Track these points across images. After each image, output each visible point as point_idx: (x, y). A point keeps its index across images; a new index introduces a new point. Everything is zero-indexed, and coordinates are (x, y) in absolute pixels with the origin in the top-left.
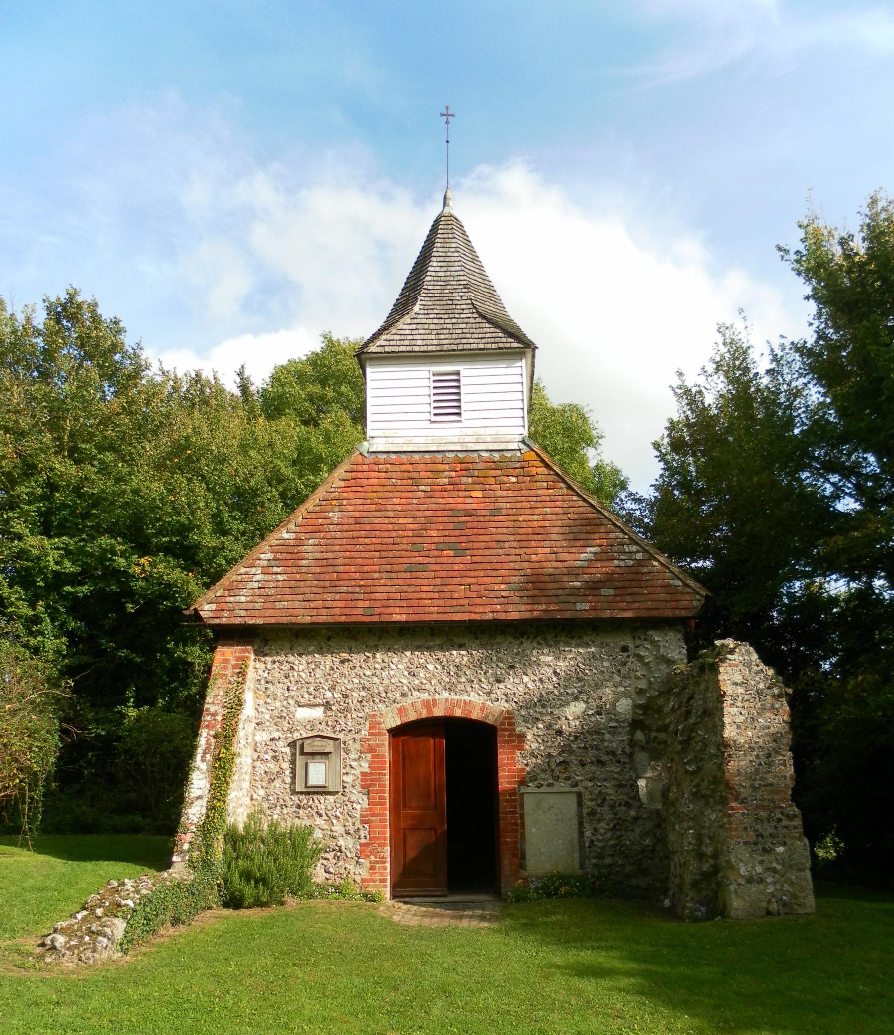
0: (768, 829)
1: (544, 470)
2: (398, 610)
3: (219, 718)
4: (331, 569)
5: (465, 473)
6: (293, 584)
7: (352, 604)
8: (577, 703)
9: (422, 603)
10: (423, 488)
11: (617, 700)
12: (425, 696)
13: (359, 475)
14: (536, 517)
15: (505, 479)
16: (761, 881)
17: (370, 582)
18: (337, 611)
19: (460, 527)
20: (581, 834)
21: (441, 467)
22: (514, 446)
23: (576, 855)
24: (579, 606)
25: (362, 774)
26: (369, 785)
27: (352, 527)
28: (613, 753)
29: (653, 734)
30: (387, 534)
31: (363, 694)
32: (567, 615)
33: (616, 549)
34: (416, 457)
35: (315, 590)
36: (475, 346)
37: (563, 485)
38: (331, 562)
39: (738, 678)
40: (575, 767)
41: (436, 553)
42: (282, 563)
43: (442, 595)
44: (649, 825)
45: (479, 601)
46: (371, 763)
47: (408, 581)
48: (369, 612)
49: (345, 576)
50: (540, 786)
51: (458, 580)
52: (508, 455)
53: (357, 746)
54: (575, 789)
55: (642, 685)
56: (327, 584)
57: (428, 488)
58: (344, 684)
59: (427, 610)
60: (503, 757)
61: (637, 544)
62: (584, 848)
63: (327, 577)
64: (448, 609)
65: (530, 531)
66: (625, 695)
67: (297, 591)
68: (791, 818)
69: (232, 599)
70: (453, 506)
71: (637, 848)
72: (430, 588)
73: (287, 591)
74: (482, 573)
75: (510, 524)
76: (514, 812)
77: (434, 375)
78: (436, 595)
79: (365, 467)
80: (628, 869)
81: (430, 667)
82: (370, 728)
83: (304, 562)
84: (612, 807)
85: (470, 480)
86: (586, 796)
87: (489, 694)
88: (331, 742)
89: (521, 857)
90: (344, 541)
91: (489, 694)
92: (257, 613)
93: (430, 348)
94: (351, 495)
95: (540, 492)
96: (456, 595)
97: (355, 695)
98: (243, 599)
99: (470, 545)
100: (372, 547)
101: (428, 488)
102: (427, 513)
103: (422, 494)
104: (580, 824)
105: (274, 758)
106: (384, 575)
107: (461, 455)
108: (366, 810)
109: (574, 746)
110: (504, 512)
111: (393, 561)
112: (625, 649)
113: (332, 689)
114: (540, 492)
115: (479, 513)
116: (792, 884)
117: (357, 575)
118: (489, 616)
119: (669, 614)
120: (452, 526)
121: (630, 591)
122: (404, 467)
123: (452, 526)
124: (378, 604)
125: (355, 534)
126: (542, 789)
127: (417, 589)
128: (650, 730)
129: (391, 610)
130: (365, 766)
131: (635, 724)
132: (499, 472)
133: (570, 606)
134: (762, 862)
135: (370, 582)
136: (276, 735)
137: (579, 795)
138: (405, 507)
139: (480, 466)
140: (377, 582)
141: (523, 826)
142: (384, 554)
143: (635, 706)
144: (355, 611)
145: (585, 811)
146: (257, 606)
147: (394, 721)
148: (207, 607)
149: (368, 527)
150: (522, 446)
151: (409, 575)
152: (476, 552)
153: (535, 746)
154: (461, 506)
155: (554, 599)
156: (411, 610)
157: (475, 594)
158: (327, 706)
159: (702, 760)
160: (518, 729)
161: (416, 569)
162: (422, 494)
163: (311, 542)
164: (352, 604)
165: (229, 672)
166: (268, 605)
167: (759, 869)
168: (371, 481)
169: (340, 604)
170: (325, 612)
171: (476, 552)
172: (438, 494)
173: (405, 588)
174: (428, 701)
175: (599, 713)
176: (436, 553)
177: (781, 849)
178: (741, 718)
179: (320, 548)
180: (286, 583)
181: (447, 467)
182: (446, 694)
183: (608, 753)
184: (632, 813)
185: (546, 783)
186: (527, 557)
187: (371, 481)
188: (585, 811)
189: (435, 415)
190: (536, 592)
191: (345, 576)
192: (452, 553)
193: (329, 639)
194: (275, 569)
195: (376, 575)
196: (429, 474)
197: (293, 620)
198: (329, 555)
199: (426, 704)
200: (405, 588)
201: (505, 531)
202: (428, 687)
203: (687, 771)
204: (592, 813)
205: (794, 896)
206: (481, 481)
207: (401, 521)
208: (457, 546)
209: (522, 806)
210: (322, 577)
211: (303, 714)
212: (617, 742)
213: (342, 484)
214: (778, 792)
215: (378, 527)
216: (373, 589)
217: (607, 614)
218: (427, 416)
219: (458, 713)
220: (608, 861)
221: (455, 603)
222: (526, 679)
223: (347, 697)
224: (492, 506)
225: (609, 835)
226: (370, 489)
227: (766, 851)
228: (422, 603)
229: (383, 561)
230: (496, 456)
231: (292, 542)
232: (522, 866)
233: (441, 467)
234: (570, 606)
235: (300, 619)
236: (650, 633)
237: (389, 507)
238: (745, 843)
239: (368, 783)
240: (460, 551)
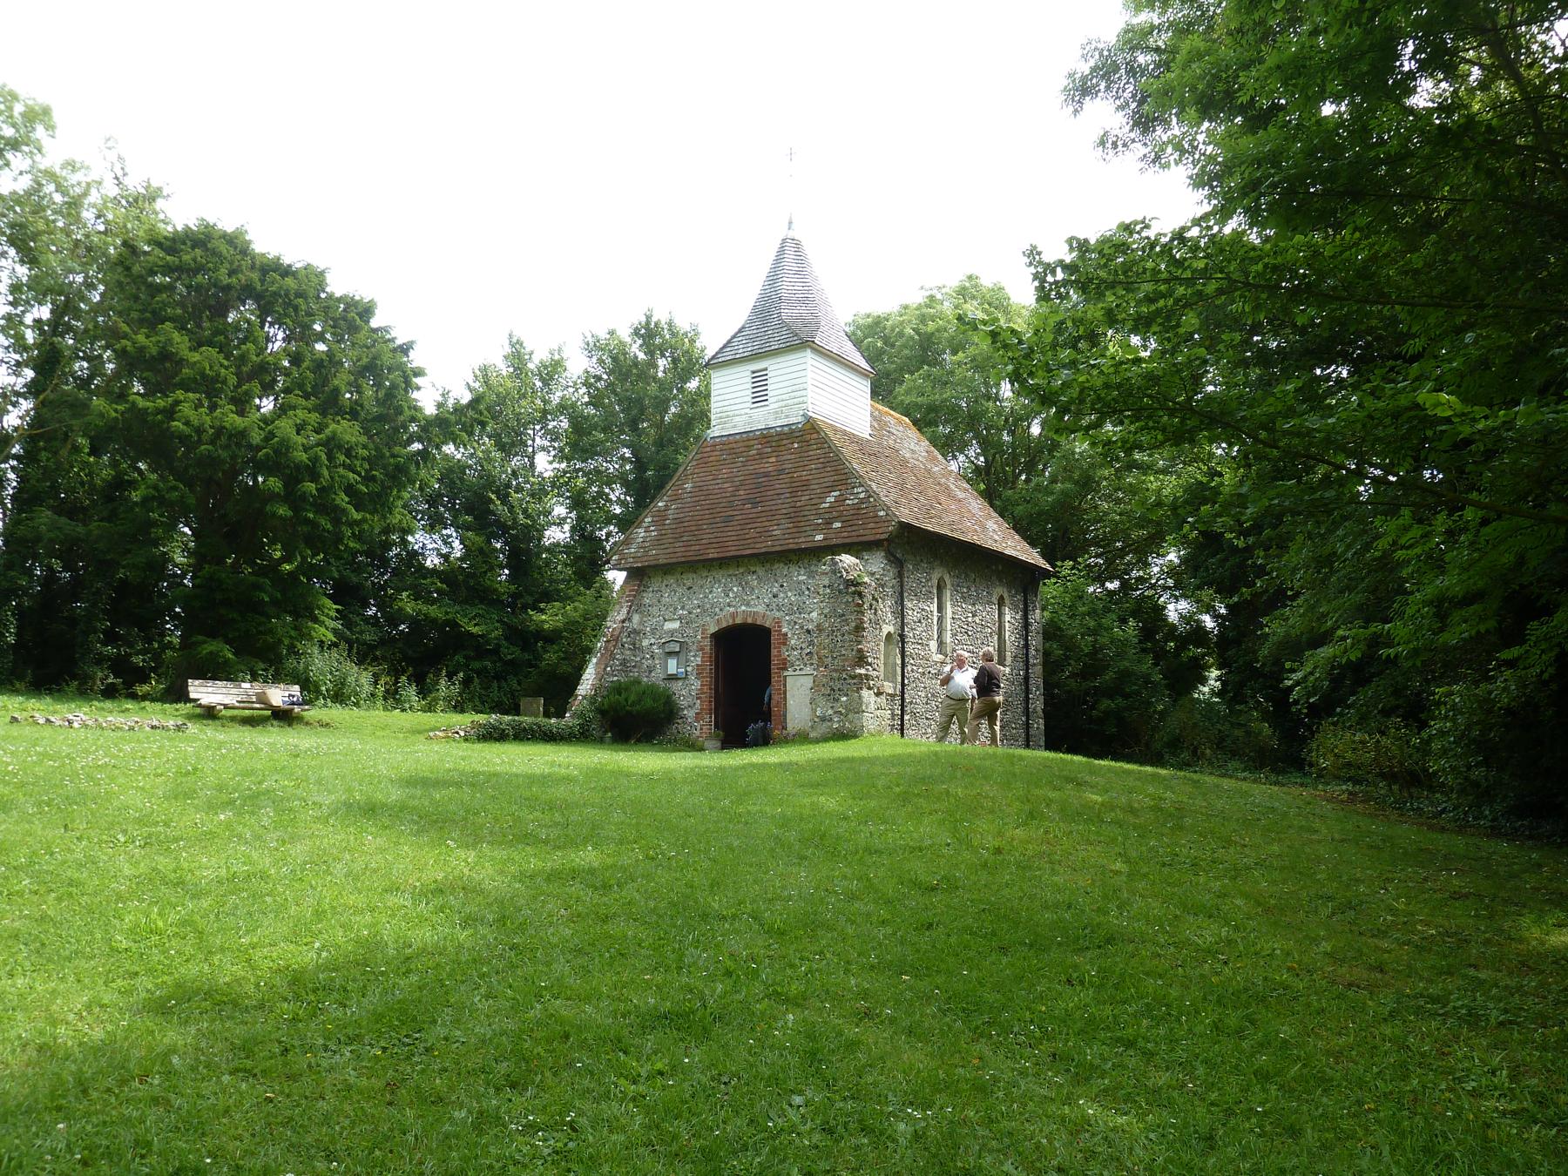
0: (837, 685)
22: (800, 419)
39: (826, 582)
60: (774, 652)
119: (871, 538)
147: (713, 629)
199: (733, 615)
211: (669, 626)
217: (834, 541)
219: (750, 621)
240: (755, 504)
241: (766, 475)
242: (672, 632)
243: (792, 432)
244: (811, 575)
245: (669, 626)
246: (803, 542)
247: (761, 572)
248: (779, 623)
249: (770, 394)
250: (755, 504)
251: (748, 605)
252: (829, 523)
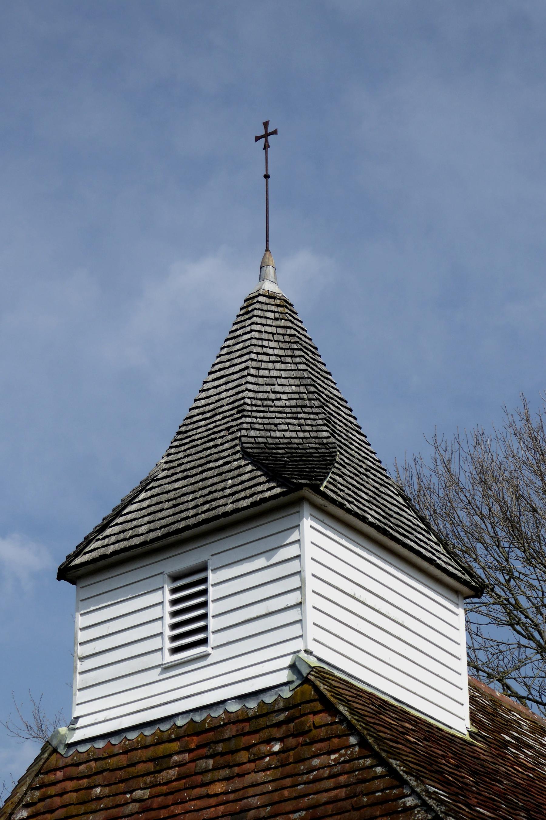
1: (324, 718)
5: (204, 751)
10: (139, 793)
13: (51, 791)
15: (265, 748)
22: (284, 677)
37: (353, 740)
52: (269, 699)
107: (198, 718)
181: (175, 746)
189: (175, 651)
196: (151, 766)
206: (226, 760)
218: (156, 659)
230: (252, 704)
243: (267, 711)
249: (213, 624)
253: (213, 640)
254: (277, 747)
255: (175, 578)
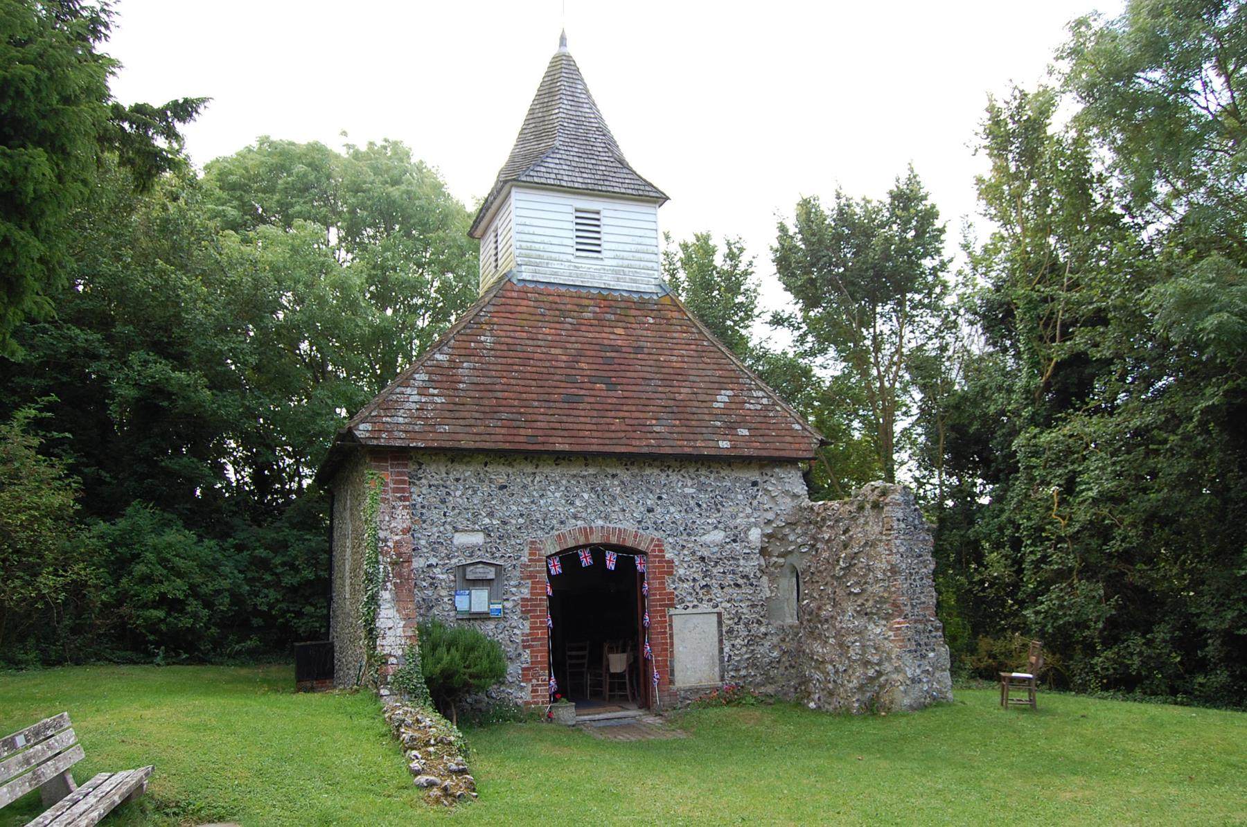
1: (675, 314)
2: (560, 440)
3: (390, 544)
4: (491, 395)
6: (451, 407)
7: (515, 431)
8: (716, 532)
9: (581, 433)
11: (749, 530)
12: (580, 523)
13: (509, 301)
14: (675, 358)
16: (920, 681)
17: (530, 410)
18: (500, 438)
19: (608, 361)
20: (721, 650)
21: (586, 302)
22: (653, 289)
23: (717, 669)
24: (721, 444)
25: (523, 599)
26: (530, 611)
27: (506, 354)
28: (746, 577)
29: (775, 559)
30: (539, 364)
31: (521, 521)
32: (713, 452)
33: (745, 393)
34: (563, 290)
35: (477, 415)
36: (617, 190)
37: (694, 330)
38: (489, 387)
39: (900, 515)
40: (716, 590)
41: (589, 386)
42: (438, 385)
43: (600, 427)
44: (775, 640)
45: (634, 435)
46: (532, 588)
47: (567, 412)
48: (533, 440)
49: (504, 402)
50: (686, 608)
51: (613, 414)
53: (517, 573)
54: (716, 610)
55: (770, 516)
56: (487, 409)
57: (574, 321)
58: (502, 512)
59: (587, 440)
61: (762, 390)
62: (724, 663)
63: (486, 402)
64: (607, 441)
65: (671, 371)
66: (756, 525)
67: (457, 415)
68: (937, 629)
69: (388, 419)
70: (600, 341)
71: (767, 660)
72: (588, 420)
73: (447, 414)
74: (634, 408)
75: (651, 363)
76: (665, 633)
77: (577, 211)
78: (594, 427)
79: (515, 295)
80: (759, 679)
81: (586, 496)
82: (530, 554)
83: (461, 386)
84: (746, 625)
85: (613, 317)
86: (725, 616)
87: (639, 522)
88: (493, 569)
89: (669, 672)
90: (499, 367)
91: (639, 522)
92: (418, 436)
93: (576, 185)
94: (502, 321)
95: (675, 335)
96: (613, 428)
97: (514, 522)
98: (401, 420)
99: (620, 380)
100: (528, 376)
101: (574, 321)
102: (576, 346)
103: (569, 327)
104: (721, 641)
105: (432, 584)
106: (544, 404)
108: (527, 635)
109: (715, 571)
110: (646, 351)
111: (550, 390)
112: (755, 484)
113: (491, 515)
114: (675, 335)
115: (624, 349)
116: (939, 682)
117: (516, 403)
118: (645, 450)
120: (600, 360)
121: (761, 432)
122: (551, 298)
123: (600, 360)
124: (540, 433)
125: (510, 361)
126: (688, 611)
127: (576, 420)
128: (771, 556)
129: (552, 440)
130: (526, 592)
131: (763, 551)
132: (638, 313)
133: (711, 444)
134: (919, 666)
135: (530, 410)
136: (433, 561)
137: (719, 615)
138: (555, 338)
139: (622, 305)
140: (536, 410)
141: (672, 644)
142: (540, 383)
143: (764, 535)
144: (517, 439)
145: (724, 629)
146: (417, 428)
148: (361, 427)
149: (521, 355)
150: (659, 290)
151: (566, 405)
152: (625, 388)
153: (681, 571)
154: (606, 342)
155: (699, 437)
156: (572, 441)
157: (629, 428)
158: (487, 531)
159: (866, 583)
160: (668, 556)
161: (573, 400)
162: (569, 327)
163: (465, 365)
164: (515, 431)
165: (390, 496)
166: (427, 428)
167: (918, 671)
168: (519, 309)
169: (503, 431)
170: (487, 438)
171: (625, 388)
172: (583, 328)
173: (564, 418)
174: (585, 529)
175: (735, 541)
176: (589, 386)
177: (931, 655)
178: (902, 549)
179: (476, 373)
180: (446, 407)
181: (592, 302)
182: (600, 522)
183: (743, 577)
184: (763, 629)
185: (691, 605)
186: (672, 396)
187: (519, 309)
188: (724, 629)
190: (684, 429)
191: (504, 402)
192: (604, 386)
193: (486, 465)
194: (431, 391)
195: (536, 404)
197: (456, 445)
198: (486, 380)
199: (584, 531)
200: (564, 418)
201: (649, 369)
202: (584, 515)
203: (851, 593)
204: (730, 631)
205: (940, 692)
207: (553, 351)
208: (607, 380)
209: (671, 626)
210: (481, 402)
211: (461, 539)
212: (750, 566)
213: (492, 309)
214: (927, 608)
215: (531, 355)
216: (535, 417)
217: (746, 452)
220: (743, 672)
221: (613, 435)
222: (672, 509)
223: (505, 523)
224: (634, 344)
225: (744, 649)
226: (519, 316)
227: (923, 657)
228: (581, 433)
229: (540, 390)
230: (636, 296)
231: (446, 364)
232: (672, 682)
233: (586, 302)
234: (711, 444)
235: (463, 444)
236: (777, 470)
237: (540, 337)
238: (910, 651)
239: (527, 609)
240: (612, 386)
241: (616, 349)
242: (471, 550)
243: (645, 302)
244: (701, 488)
245: (461, 539)
246: (702, 446)
247: (625, 475)
248: (660, 545)
250: (612, 386)
251: (606, 518)
252: (731, 427)
253: (605, 254)
254: (651, 321)
255: (577, 211)
